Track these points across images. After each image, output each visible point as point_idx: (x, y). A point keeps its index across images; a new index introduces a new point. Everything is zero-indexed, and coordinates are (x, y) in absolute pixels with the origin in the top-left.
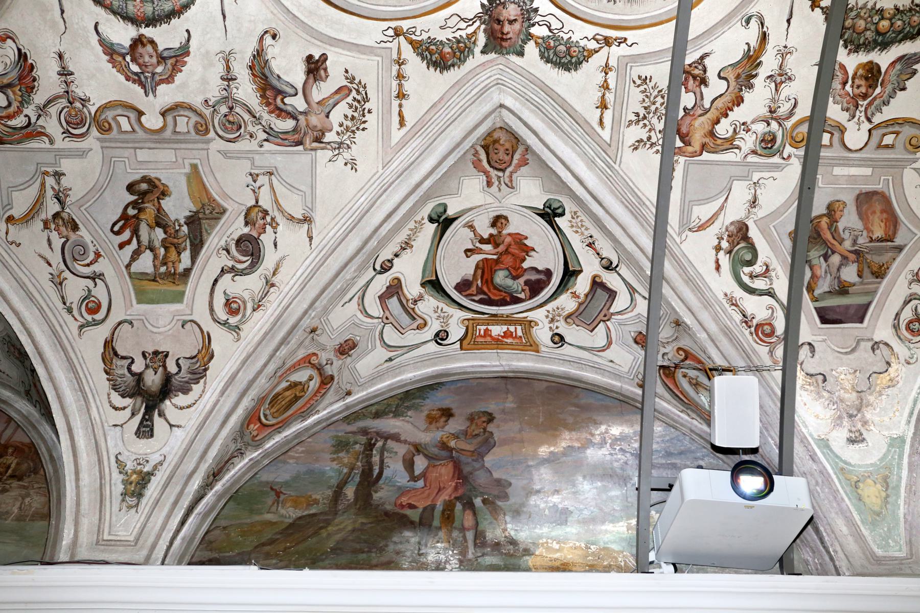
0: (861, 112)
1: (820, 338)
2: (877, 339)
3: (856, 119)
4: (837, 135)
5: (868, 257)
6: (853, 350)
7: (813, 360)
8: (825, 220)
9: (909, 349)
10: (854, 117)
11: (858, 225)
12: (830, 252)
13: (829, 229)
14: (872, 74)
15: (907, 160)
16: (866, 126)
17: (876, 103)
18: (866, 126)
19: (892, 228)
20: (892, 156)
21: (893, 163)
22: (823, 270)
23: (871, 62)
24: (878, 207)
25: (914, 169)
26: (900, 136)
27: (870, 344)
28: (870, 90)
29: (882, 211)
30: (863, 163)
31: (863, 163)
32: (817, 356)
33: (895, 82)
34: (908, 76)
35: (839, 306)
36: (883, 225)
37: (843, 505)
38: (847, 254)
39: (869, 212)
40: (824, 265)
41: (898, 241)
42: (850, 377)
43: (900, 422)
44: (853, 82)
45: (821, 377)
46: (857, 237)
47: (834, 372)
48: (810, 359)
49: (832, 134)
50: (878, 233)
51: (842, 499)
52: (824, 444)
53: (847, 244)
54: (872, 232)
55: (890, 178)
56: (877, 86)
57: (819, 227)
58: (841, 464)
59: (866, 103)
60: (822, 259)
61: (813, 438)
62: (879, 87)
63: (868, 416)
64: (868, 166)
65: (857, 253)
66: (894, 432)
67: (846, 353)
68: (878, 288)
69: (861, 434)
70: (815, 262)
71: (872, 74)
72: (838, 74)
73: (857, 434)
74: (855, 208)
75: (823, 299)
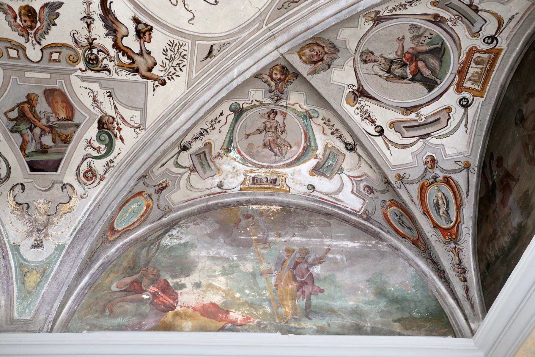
0: (32, 38)
1: (29, 181)
2: (65, 182)
3: (30, 41)
4: (21, 52)
5: (57, 129)
6: (50, 189)
7: (23, 194)
8: (27, 106)
9: (84, 189)
10: (28, 41)
11: (49, 110)
12: (33, 126)
13: (31, 111)
14: (31, 13)
15: (71, 70)
16: (38, 47)
17: (40, 32)
18: (38, 47)
19: (70, 112)
20: (60, 67)
21: (62, 71)
22: (30, 138)
23: (27, 6)
24: (59, 99)
25: (77, 76)
26: (62, 54)
27: (61, 185)
28: (34, 24)
29: (62, 102)
30: (42, 70)
31: (43, 70)
32: (25, 192)
33: (47, 20)
34: (55, 17)
35: (42, 161)
36: (64, 110)
37: (11, 288)
38: (44, 128)
39: (54, 102)
40: (30, 134)
41: (76, 121)
42: (45, 206)
43: (66, 235)
44: (21, 18)
45: (26, 205)
46: (49, 117)
47: (35, 203)
48: (20, 194)
49: (18, 51)
50: (62, 115)
51: (12, 283)
52: (16, 248)
53: (44, 121)
54: (58, 114)
55: (63, 81)
56: (37, 22)
57: (24, 110)
58: (22, 261)
59: (33, 32)
60: (28, 130)
61: (9, 243)
62: (39, 22)
63: (50, 231)
64: (47, 73)
65: (50, 127)
66: (61, 241)
67: (45, 191)
68: (66, 150)
69: (42, 242)
70: (24, 132)
71: (31, 13)
72: (9, 12)
73: (39, 242)
74: (44, 99)
75: (32, 156)
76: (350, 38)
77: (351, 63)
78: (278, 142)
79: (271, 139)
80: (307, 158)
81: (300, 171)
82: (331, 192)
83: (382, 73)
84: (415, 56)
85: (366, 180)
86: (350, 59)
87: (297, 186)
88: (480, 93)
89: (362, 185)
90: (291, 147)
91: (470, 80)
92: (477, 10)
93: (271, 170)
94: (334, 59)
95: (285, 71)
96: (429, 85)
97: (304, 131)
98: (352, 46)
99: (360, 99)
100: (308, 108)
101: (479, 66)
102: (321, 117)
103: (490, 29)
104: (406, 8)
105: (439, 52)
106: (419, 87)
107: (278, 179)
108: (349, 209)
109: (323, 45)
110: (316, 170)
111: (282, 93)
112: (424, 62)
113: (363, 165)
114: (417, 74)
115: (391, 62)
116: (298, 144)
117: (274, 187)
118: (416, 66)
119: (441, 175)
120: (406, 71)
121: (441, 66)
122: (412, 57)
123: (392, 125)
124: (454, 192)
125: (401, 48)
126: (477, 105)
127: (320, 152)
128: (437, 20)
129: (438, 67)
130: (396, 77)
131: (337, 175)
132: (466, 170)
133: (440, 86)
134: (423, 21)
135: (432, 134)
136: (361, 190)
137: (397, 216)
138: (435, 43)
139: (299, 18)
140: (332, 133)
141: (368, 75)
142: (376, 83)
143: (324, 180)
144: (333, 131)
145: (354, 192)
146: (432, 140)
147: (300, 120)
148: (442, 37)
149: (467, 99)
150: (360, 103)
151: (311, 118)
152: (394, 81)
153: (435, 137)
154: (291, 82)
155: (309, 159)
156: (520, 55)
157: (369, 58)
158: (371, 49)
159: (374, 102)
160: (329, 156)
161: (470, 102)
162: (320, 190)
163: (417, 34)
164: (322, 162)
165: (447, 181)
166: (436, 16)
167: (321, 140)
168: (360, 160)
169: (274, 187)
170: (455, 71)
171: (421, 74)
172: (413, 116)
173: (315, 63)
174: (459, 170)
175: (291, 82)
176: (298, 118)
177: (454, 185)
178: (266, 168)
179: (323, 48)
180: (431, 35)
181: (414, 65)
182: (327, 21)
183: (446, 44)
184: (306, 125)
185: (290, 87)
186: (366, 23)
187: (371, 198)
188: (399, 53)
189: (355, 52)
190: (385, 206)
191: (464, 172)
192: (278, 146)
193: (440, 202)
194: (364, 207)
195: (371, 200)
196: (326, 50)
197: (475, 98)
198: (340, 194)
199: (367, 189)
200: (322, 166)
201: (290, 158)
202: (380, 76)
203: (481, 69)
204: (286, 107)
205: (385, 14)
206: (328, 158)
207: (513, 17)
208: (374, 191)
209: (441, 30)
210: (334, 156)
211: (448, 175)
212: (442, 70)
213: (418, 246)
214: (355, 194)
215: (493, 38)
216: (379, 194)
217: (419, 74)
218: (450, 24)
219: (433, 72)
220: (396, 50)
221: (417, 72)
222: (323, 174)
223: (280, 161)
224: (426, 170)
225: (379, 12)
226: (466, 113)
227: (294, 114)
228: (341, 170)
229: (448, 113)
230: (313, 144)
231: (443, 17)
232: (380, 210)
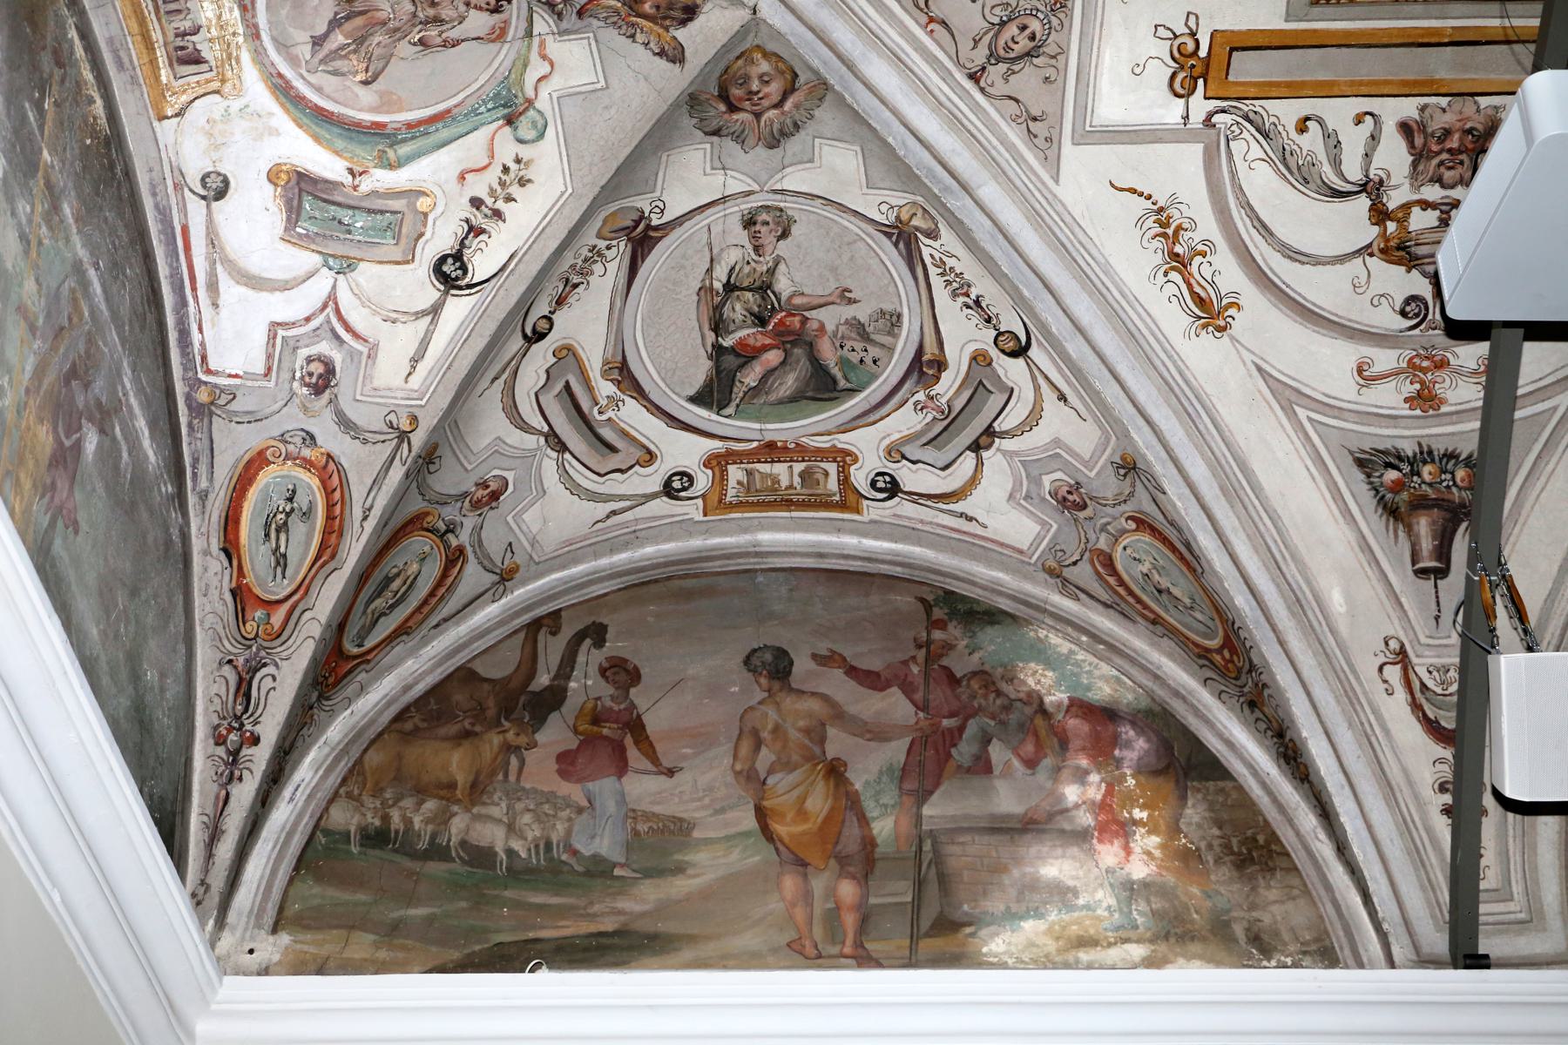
76: (829, 168)
77: (735, 186)
78: (377, 39)
79: (382, 15)
80: (340, 144)
81: (275, 132)
82: (232, 256)
83: (721, 273)
84: (796, 339)
85: (352, 355)
86: (749, 181)
87: (203, 141)
88: (716, 503)
89: (325, 347)
90: (366, 83)
91: (749, 473)
92: (976, 447)
93: (241, 39)
94: (740, 138)
95: (678, 14)
96: (711, 392)
97: (448, 111)
98: (794, 180)
99: (622, 244)
100: (543, 103)
101: (797, 480)
102: (525, 152)
103: (912, 478)
104: (954, 294)
105: (823, 387)
106: (700, 371)
107: (204, 67)
108: (196, 337)
109: (788, 106)
110: (299, 189)
111: (580, 14)
112: (783, 363)
113: (410, 334)
114: (738, 355)
115: (764, 288)
116: (388, 102)
117: (162, 60)
118: (765, 348)
119: (464, 537)
120: (742, 328)
121: (780, 402)
122: (790, 333)
123: (564, 352)
124: (432, 594)
125: (816, 302)
126: (679, 510)
127: (381, 179)
128: (926, 367)
129: (773, 397)
130: (718, 309)
131: (318, 259)
132: (496, 578)
133: (714, 417)
134: (916, 338)
135: (567, 456)
136: (304, 353)
137: (290, 500)
138: (852, 376)
139: (870, 23)
140: (476, 203)
141: (705, 241)
142: (683, 267)
143: (275, 219)
144: (489, 201)
145: (281, 333)
146: (549, 464)
147: (487, 88)
148: (873, 386)
149: (691, 485)
150: (608, 248)
151: (510, 121)
152: (703, 308)
153: (562, 467)
154: (633, 36)
155: (337, 153)
156: (869, 560)
157: (764, 229)
158: (795, 230)
159: (623, 280)
160: (382, 212)
161: (683, 494)
162: (219, 218)
163: (870, 329)
164: (346, 195)
165: (455, 558)
166: (940, 365)
167: (436, 176)
168: (424, 313)
169: (162, 60)
170: (769, 437)
171: (742, 366)
172: (605, 389)
173: (724, 96)
174: (490, 566)
175: (633, 36)
176: (495, 82)
177: (451, 579)
178: (243, 18)
179: (779, 105)
180: (875, 362)
181: (768, 341)
182: (888, 114)
183: (851, 398)
184: (475, 112)
185: (612, 36)
186: (884, 208)
187: (293, 394)
188: (797, 301)
189: (775, 192)
190: (291, 447)
191: (491, 578)
192: (360, 41)
193: (395, 585)
194: (238, 381)
195: (285, 395)
196: (772, 113)
197: (700, 502)
198: (242, 290)
199: (317, 368)
200: (325, 201)
201: (319, 90)
202: (710, 271)
203: (791, 487)
204: (529, 33)
205: (926, 252)
206: (370, 211)
207: (970, 519)
208: (327, 395)
209: (894, 380)
210: (394, 229)
211: (469, 550)
212: (766, 409)
213: (241, 615)
214: (272, 337)
215: (893, 489)
216: (328, 415)
217: (742, 360)
218: (921, 396)
219: (754, 391)
220: (806, 291)
221: (746, 354)
222: (293, 213)
223: (293, 61)
224: (465, 495)
225: (933, 234)
226: (654, 496)
227: (508, 64)
228: (346, 266)
229: (637, 463)
230: (404, 150)
231: (938, 379)
232: (267, 435)
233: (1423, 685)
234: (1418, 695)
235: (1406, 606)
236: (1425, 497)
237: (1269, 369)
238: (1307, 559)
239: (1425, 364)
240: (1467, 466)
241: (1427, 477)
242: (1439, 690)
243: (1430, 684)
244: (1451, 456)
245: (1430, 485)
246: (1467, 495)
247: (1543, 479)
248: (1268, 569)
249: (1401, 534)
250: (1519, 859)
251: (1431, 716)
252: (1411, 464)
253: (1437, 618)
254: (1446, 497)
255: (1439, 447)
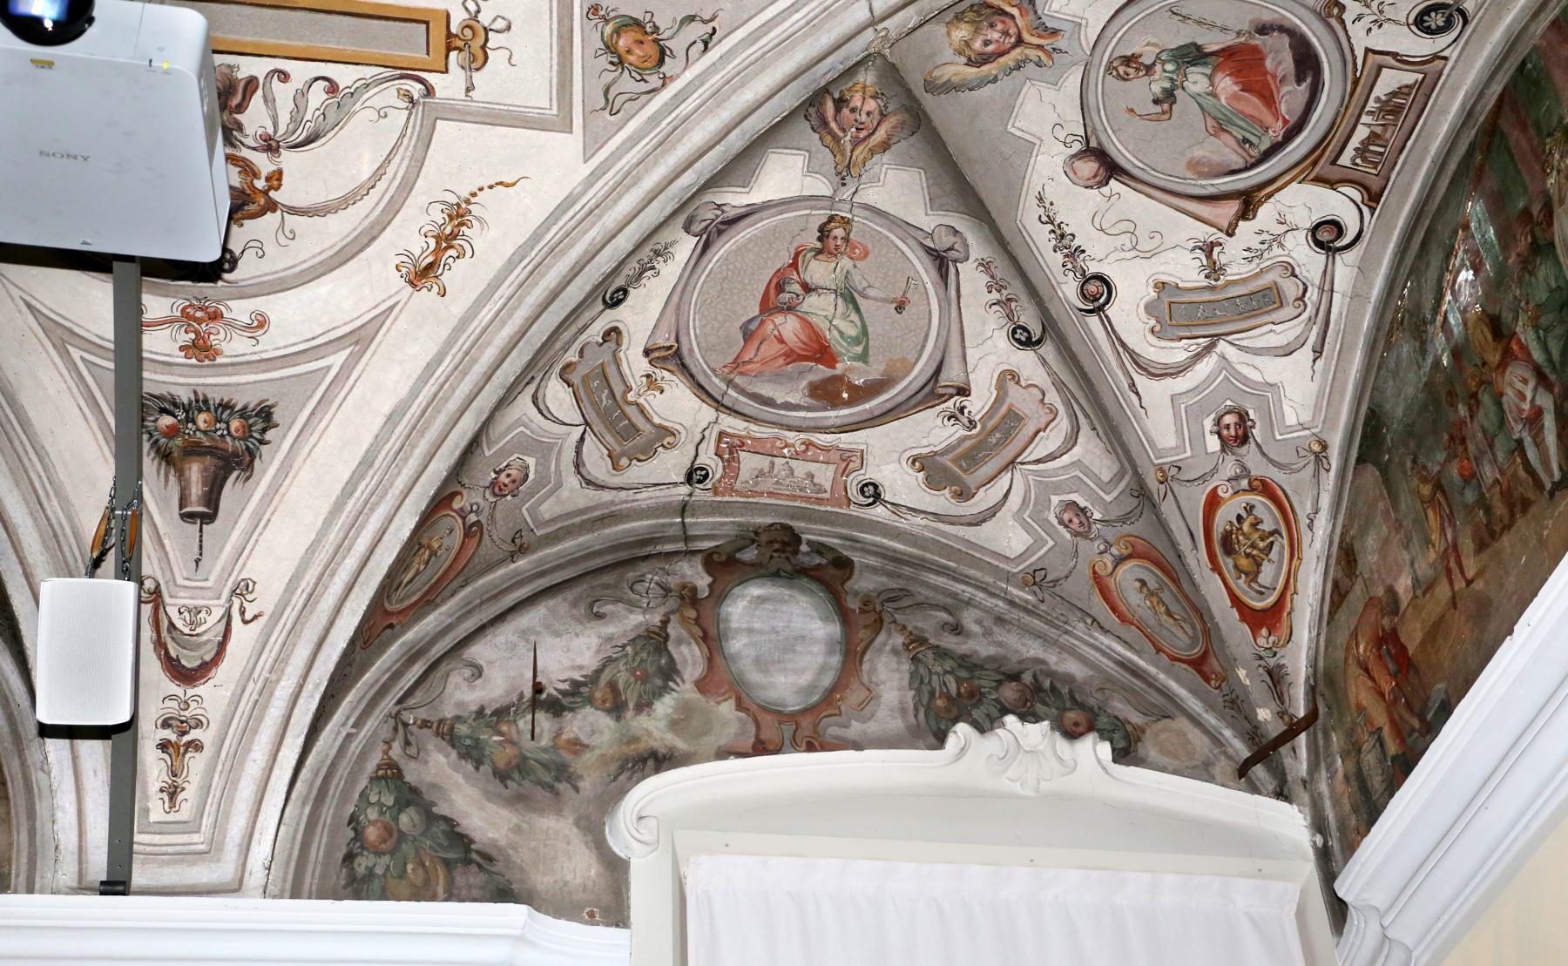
233: (172, 625)
234: (164, 633)
235: (168, 548)
236: (199, 444)
237: (38, 306)
238: (72, 497)
239: (199, 314)
240: (241, 417)
241: (202, 425)
242: (186, 631)
243: (179, 624)
244: (226, 406)
245: (205, 433)
246: (241, 445)
247: (316, 435)
248: (27, 504)
249: (172, 478)
250: (218, 794)
251: (173, 654)
252: (187, 411)
253: (197, 561)
254: (220, 445)
255: (215, 397)
